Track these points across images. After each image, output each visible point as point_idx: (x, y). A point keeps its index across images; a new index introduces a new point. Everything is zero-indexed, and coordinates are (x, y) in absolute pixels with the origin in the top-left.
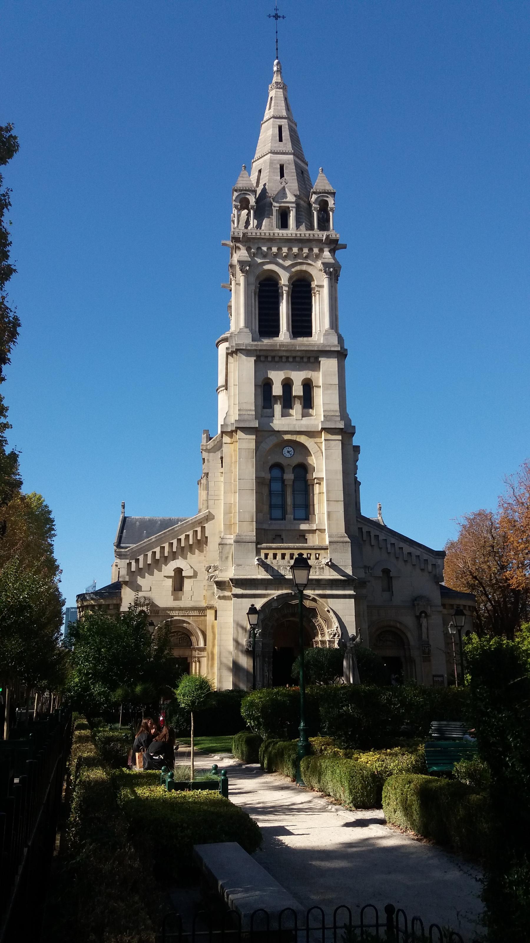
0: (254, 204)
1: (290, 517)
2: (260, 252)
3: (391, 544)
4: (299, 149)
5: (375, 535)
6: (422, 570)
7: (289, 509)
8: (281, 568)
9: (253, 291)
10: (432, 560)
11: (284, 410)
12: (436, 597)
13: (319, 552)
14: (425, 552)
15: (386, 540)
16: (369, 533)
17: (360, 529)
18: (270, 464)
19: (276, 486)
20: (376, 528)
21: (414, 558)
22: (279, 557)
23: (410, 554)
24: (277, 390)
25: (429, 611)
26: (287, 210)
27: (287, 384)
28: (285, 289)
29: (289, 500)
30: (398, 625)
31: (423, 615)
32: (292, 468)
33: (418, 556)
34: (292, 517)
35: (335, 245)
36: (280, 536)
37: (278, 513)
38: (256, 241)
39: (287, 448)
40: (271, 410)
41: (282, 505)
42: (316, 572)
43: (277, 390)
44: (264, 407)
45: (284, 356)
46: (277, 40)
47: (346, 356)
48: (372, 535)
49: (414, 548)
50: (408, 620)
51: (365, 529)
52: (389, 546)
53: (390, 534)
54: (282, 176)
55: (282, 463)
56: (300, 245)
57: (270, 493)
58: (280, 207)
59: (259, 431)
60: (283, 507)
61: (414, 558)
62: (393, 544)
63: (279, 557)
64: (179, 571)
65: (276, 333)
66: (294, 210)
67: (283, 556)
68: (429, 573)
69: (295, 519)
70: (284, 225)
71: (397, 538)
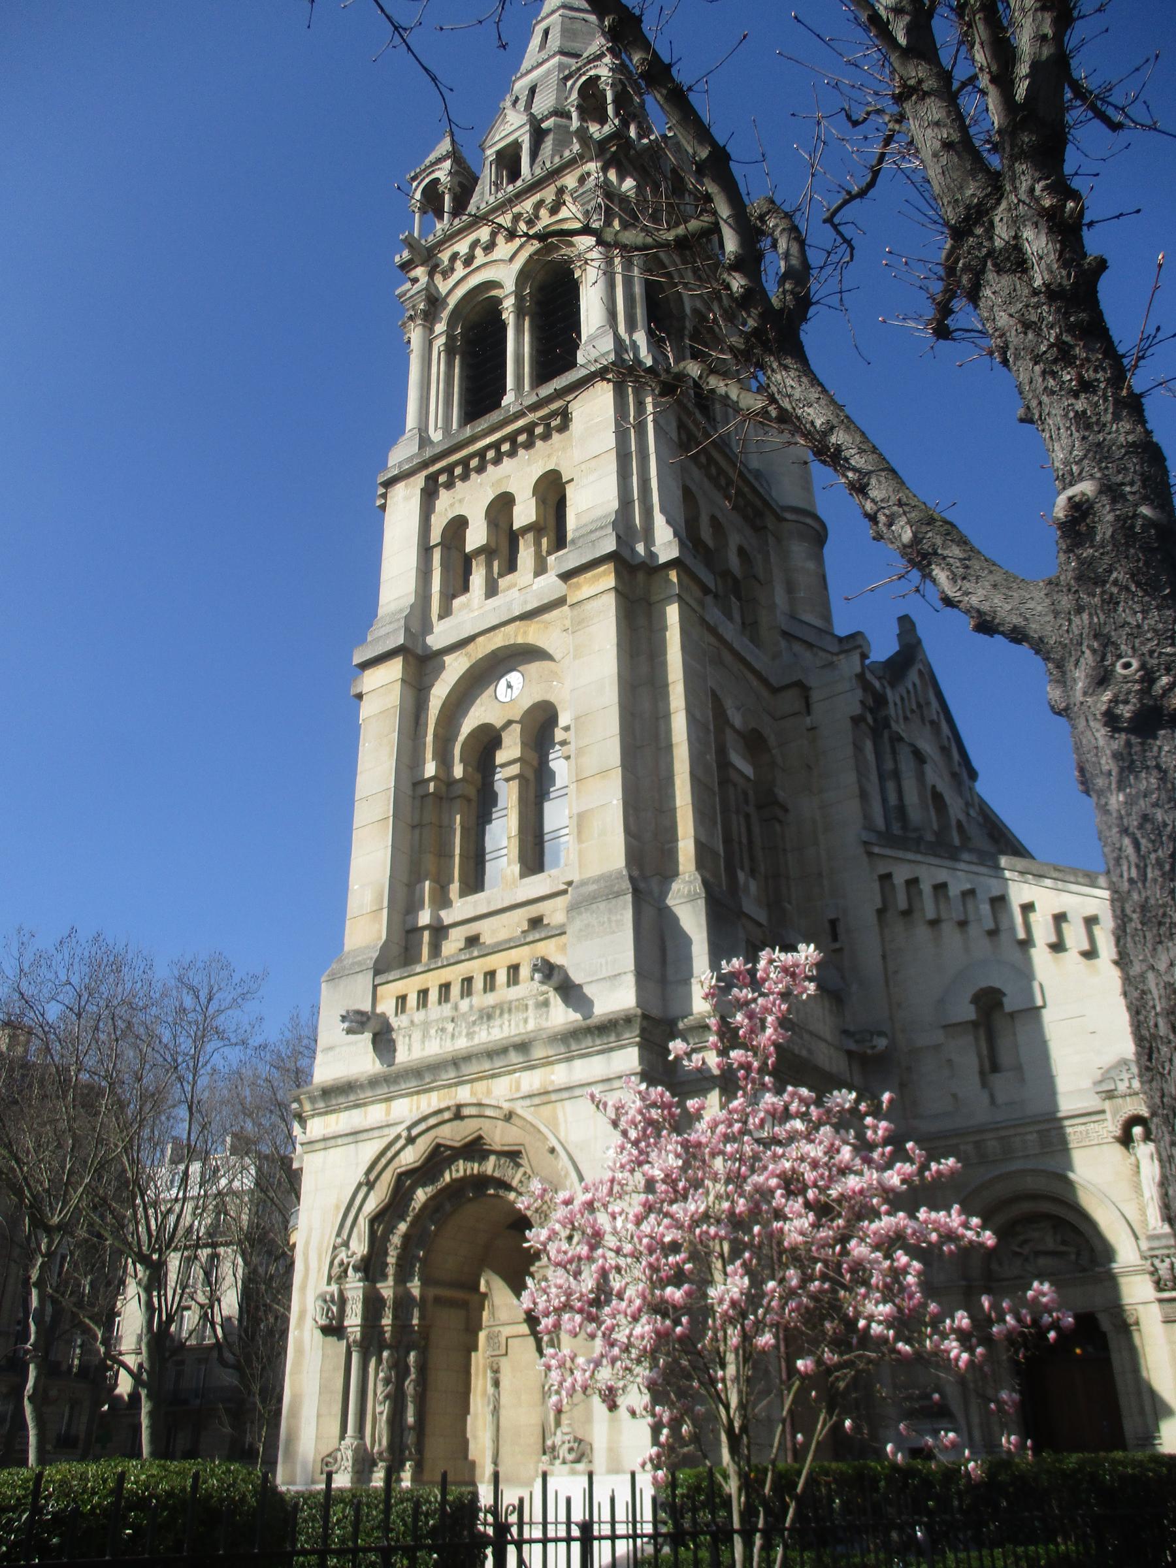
24: (476, 536)
42: (526, 1021)
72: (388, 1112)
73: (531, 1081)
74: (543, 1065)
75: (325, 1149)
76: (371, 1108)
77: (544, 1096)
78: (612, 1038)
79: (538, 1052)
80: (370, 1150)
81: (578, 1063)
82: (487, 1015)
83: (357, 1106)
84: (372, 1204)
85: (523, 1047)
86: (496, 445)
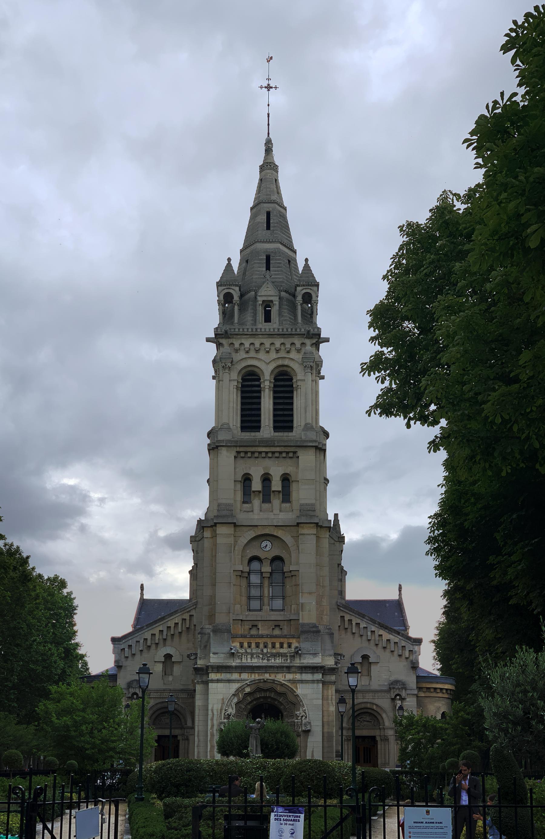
0: (238, 299)
1: (266, 608)
2: (242, 348)
3: (371, 631)
4: (286, 236)
5: (356, 623)
6: (400, 656)
7: (266, 600)
8: (255, 656)
9: (235, 387)
10: (409, 647)
11: (263, 505)
12: (412, 681)
13: (291, 641)
14: (404, 639)
15: (366, 627)
16: (350, 621)
17: (343, 617)
18: (250, 556)
19: (255, 579)
20: (357, 616)
21: (392, 644)
22: (253, 645)
23: (388, 640)
24: (256, 485)
25: (403, 694)
26: (271, 304)
27: (266, 479)
28: (267, 383)
29: (266, 594)
30: (375, 707)
31: (398, 697)
32: (269, 562)
33: (396, 643)
34: (268, 608)
35: (317, 340)
36: (256, 626)
37: (255, 604)
38: (239, 337)
39: (265, 541)
40: (250, 505)
41: (261, 596)
42: (287, 660)
43: (256, 485)
44: (244, 502)
45: (263, 452)
46: (268, 114)
47: (325, 450)
48: (354, 623)
49: (392, 635)
50: (384, 703)
51: (347, 618)
52: (369, 633)
53: (370, 623)
54: (268, 268)
55: (260, 556)
56: (282, 340)
57: (249, 585)
58: (263, 301)
59: (238, 526)
60: (261, 598)
61: (392, 644)
62: (373, 632)
63: (253, 645)
64: (168, 657)
65: (257, 428)
66: (277, 303)
67: (257, 645)
68: (407, 658)
69: (272, 610)
70: (268, 318)
71: (377, 626)
72: (240, 676)
73: (289, 676)
74: (293, 673)
75: (217, 683)
76: (233, 674)
77: (294, 681)
78: (316, 670)
79: (293, 670)
80: (236, 686)
81: (304, 675)
82: (275, 656)
83: (229, 673)
84: (235, 700)
85: (289, 668)
86: (267, 453)
